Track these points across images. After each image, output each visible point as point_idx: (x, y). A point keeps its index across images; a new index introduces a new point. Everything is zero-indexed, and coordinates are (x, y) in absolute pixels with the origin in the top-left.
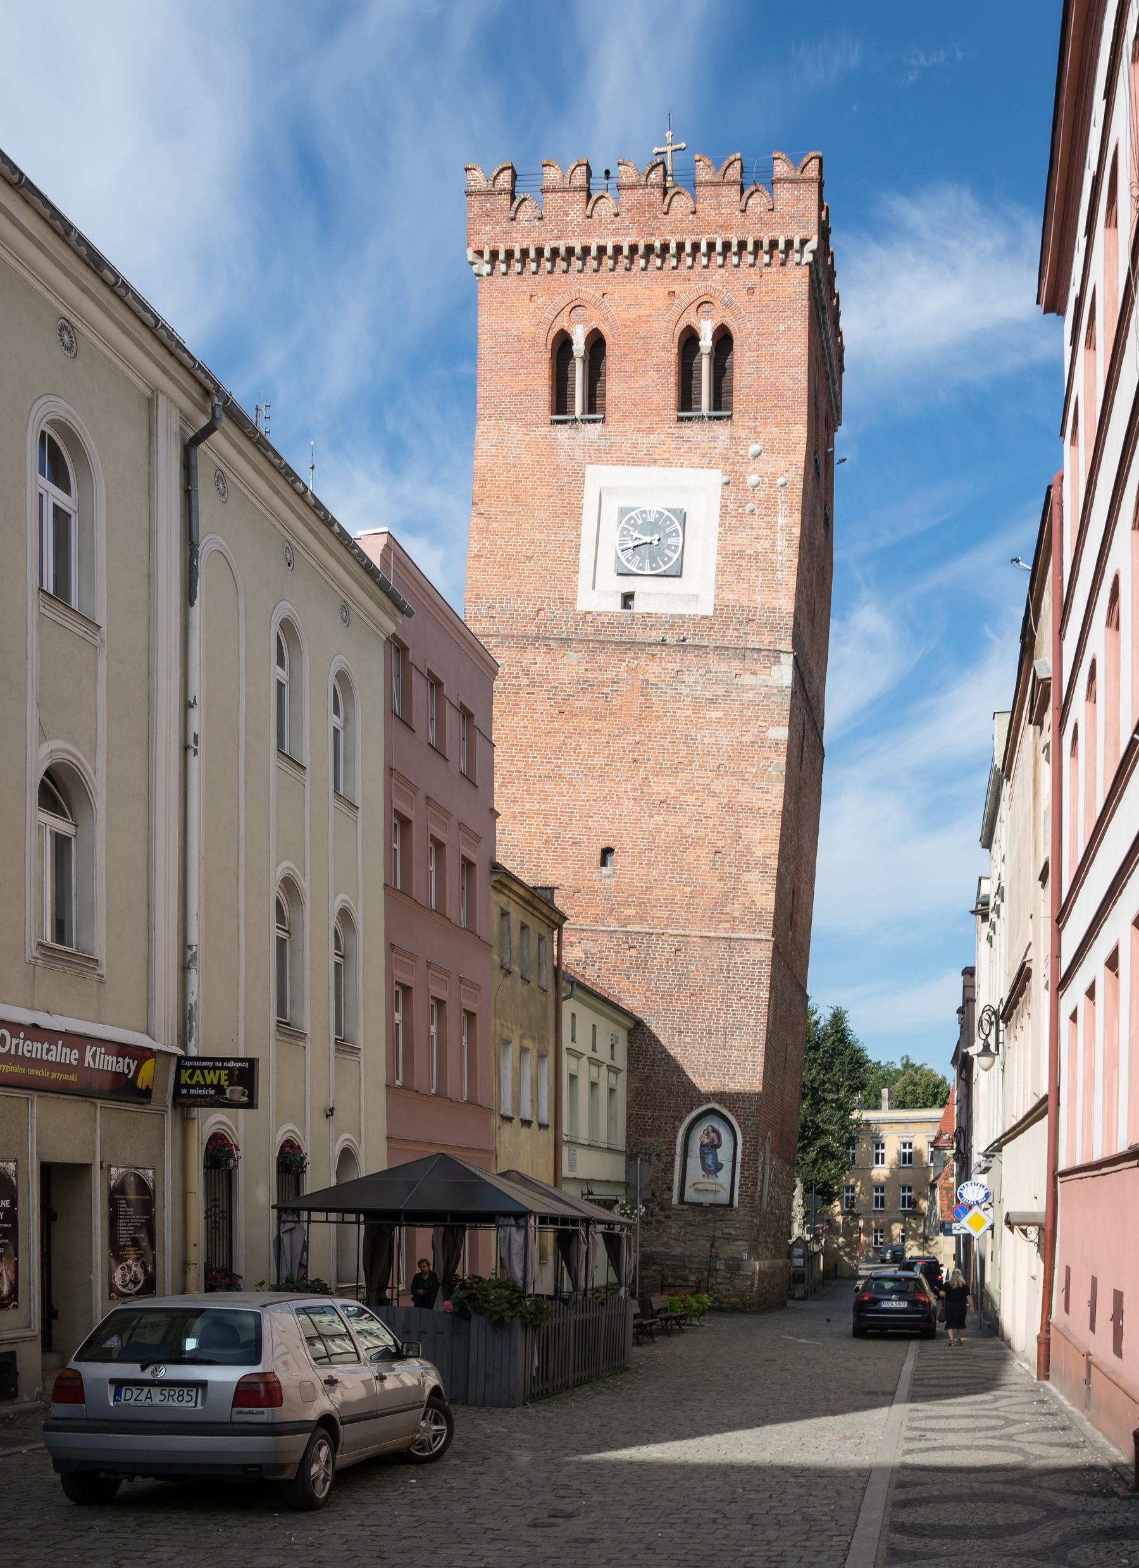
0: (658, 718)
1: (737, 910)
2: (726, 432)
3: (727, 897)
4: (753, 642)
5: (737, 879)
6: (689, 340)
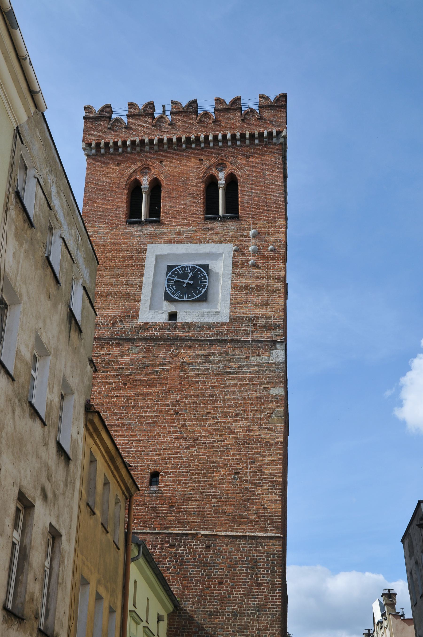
2: (235, 224)
5: (252, 491)
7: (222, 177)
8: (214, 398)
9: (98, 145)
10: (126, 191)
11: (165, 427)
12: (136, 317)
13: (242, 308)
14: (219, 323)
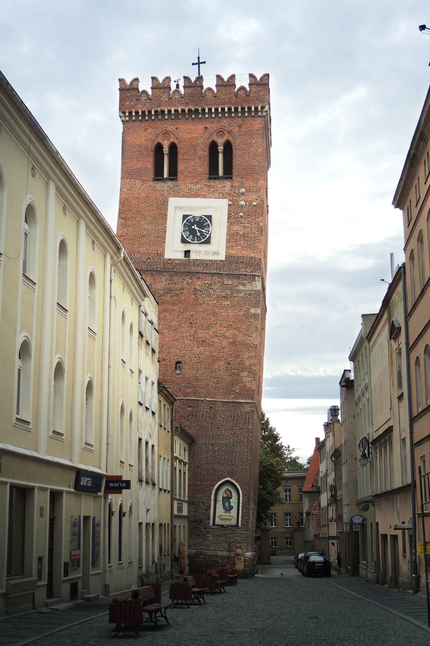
0: (201, 304)
1: (237, 389)
2: (230, 184)
3: (233, 383)
4: (243, 271)
5: (238, 375)
6: (213, 146)
7: (220, 142)
8: (214, 314)
9: (130, 113)
10: (152, 153)
11: (184, 333)
12: (162, 255)
13: (233, 250)
14: (218, 260)
